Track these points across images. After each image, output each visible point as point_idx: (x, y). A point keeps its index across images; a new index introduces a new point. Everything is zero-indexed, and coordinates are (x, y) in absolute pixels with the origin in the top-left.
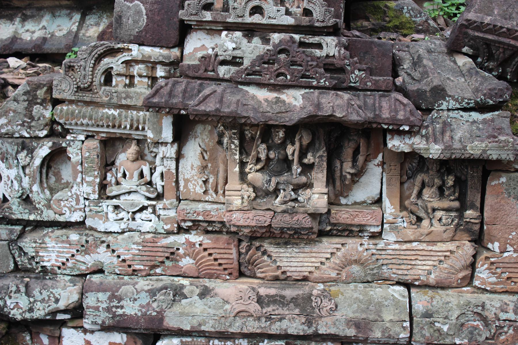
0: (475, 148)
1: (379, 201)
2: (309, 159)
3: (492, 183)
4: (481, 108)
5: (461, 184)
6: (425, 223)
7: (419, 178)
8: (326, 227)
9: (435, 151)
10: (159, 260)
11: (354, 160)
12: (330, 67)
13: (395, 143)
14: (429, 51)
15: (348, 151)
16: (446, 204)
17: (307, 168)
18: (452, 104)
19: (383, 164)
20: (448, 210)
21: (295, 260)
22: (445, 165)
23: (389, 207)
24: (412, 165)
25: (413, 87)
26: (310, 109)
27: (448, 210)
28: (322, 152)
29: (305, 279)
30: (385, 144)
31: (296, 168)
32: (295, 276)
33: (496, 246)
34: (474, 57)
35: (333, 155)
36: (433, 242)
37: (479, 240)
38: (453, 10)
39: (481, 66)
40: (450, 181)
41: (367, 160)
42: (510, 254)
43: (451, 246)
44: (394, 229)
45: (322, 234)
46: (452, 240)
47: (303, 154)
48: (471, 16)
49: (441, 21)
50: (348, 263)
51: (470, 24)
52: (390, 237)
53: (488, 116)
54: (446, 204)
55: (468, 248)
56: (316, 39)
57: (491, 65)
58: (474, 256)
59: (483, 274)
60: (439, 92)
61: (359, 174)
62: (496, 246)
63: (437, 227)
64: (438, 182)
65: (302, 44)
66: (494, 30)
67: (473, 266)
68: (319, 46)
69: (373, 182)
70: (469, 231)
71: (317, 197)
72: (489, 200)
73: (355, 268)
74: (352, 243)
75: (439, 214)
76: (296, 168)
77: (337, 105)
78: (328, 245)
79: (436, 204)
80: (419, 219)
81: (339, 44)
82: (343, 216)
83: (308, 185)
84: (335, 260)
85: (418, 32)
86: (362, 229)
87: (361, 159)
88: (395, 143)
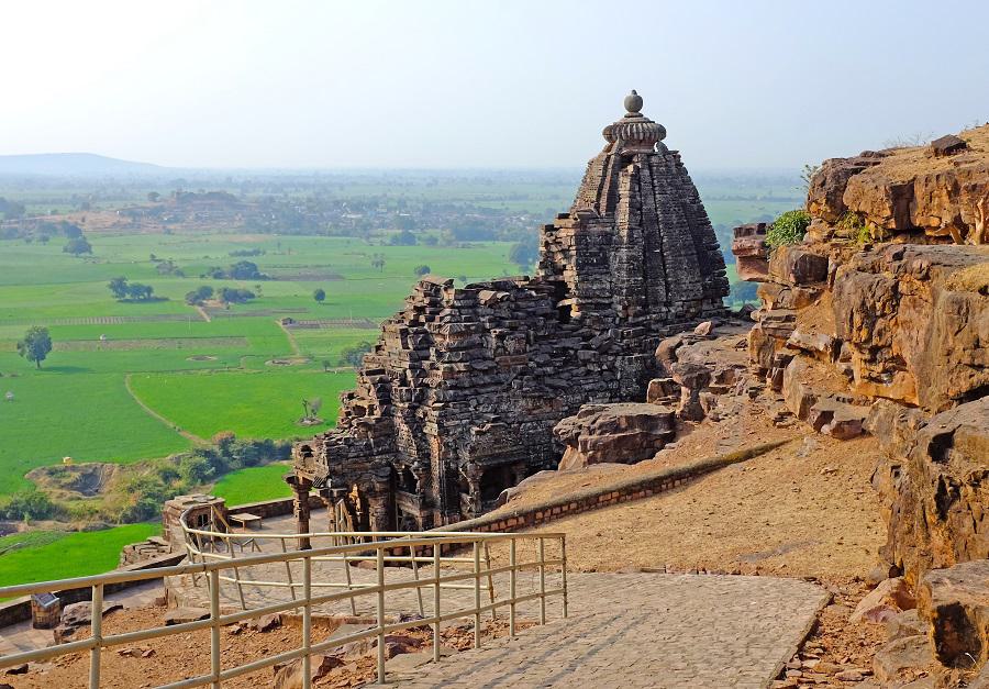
8: (539, 407)
10: (521, 414)
21: (535, 412)
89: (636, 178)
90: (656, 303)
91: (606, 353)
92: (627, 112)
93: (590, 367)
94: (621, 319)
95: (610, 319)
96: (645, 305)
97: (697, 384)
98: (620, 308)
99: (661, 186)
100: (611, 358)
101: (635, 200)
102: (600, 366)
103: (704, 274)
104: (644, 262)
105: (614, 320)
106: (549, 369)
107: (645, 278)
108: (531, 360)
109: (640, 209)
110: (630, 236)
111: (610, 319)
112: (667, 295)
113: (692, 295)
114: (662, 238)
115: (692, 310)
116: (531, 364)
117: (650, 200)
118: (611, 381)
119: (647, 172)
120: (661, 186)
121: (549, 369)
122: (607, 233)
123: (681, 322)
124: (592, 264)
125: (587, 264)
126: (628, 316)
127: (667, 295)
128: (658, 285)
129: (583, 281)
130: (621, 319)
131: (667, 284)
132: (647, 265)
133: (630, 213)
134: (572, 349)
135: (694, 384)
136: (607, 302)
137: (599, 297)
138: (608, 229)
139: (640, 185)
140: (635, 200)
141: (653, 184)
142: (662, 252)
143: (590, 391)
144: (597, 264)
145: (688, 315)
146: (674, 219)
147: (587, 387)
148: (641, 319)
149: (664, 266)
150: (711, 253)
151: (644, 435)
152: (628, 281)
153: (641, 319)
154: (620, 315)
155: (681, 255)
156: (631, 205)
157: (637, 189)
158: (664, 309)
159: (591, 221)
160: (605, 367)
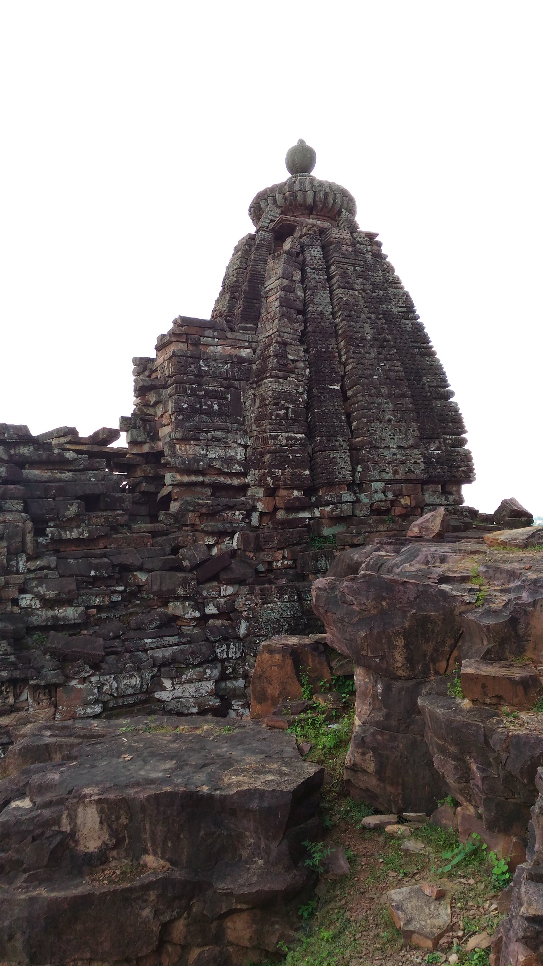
0: (53, 681)
1: (27, 700)
2: (8, 690)
3: (58, 690)
4: (54, 670)
5: (50, 691)
6: (41, 704)
7: (38, 691)
8: (13, 709)
9: (43, 683)
11: (20, 688)
12: (12, 664)
13: (32, 682)
14: (38, 655)
15: (18, 687)
16: (46, 697)
17: (8, 692)
18: (46, 670)
19: (28, 689)
20: (47, 699)
22: (45, 687)
23: (30, 701)
24: (36, 687)
25: (35, 666)
26: (10, 676)
27: (47, 699)
28: (12, 687)
29: (7, 726)
30: (29, 683)
31: (5, 693)
32: (4, 726)
33: (60, 707)
34: (50, 656)
35: (15, 688)
36: (44, 709)
37: (56, 707)
38: (42, 640)
39: (53, 658)
40: (47, 691)
41: (24, 688)
42: (65, 709)
43: (48, 709)
44: (32, 707)
45: (12, 712)
46: (48, 707)
47: (6, 689)
48: (49, 645)
49: (39, 643)
50: (19, 719)
51: (49, 648)
52: (31, 709)
53: (56, 672)
54: (46, 697)
55: (53, 709)
56: (8, 657)
57: (55, 657)
58: (55, 711)
59: (58, 716)
60: (43, 667)
61: (22, 692)
62: (60, 707)
63: (44, 704)
64: (43, 692)
65: (4, 658)
66: (55, 648)
67: (55, 714)
68: (9, 658)
69: (26, 695)
70: (53, 704)
71: (11, 700)
72: (58, 695)
73: (22, 720)
74: (20, 713)
75: (45, 701)
76: (5, 693)
77: (17, 674)
78: (13, 715)
79: (43, 698)
80: (39, 703)
81: (15, 657)
82: (18, 705)
83: (8, 697)
84: (16, 719)
85: (33, 649)
86: (23, 708)
87: (22, 688)
88: (32, 682)
89: (297, 258)
90: (331, 484)
91: (215, 578)
92: (290, 175)
93: (174, 608)
94: (262, 514)
95: (238, 515)
96: (310, 491)
97: (410, 661)
98: (260, 492)
99: (344, 275)
100: (230, 590)
101: (292, 296)
102: (200, 606)
103: (426, 437)
104: (308, 407)
105: (248, 516)
106: (70, 613)
107: (310, 434)
108: (23, 591)
109: (303, 312)
110: (281, 356)
111: (238, 515)
112: (354, 470)
113: (402, 470)
114: (345, 365)
115: (405, 501)
116: (26, 600)
117: (322, 297)
118: (225, 640)
119: (316, 252)
120: (344, 275)
121: (70, 613)
122: (241, 360)
123: (383, 522)
124: (210, 412)
125: (200, 411)
126: (276, 509)
127: (354, 470)
128: (333, 449)
129: (185, 440)
130: (262, 514)
131: (354, 449)
132: (322, 413)
133: (283, 316)
134: (141, 569)
135: (399, 657)
136: (236, 482)
137: (220, 473)
138: (245, 353)
139: (303, 272)
140: (292, 296)
141: (328, 273)
142: (343, 391)
143: (165, 663)
144: (220, 413)
145: (398, 510)
146: (368, 332)
147: (159, 654)
148: (301, 515)
149: (348, 416)
150: (439, 403)
151: (179, 894)
152: (275, 438)
153: (301, 515)
154: (260, 506)
155: (379, 395)
156: (284, 303)
157: (297, 277)
158: (348, 497)
159: (209, 332)
160: (211, 609)
